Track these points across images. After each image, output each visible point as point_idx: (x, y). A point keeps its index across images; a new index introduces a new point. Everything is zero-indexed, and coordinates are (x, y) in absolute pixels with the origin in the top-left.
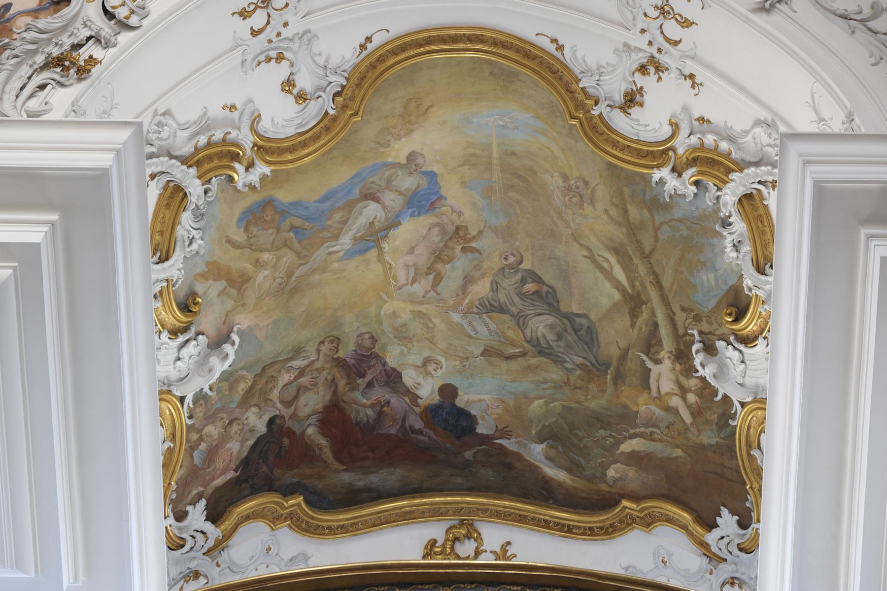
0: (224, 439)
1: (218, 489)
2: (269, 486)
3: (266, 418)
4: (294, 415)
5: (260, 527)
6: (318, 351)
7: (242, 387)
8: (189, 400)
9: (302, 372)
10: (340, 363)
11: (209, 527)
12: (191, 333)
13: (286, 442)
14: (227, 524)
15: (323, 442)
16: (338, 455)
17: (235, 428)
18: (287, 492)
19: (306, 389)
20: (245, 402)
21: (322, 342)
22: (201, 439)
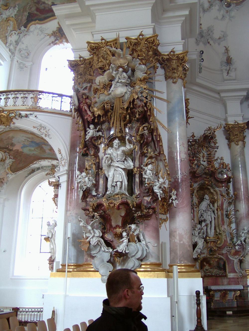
0: (22, 18)
1: (24, 24)
2: (32, 20)
3: (28, 13)
4: (31, 11)
5: (34, 26)
6: (31, 2)
7: (22, 11)
8: (14, 16)
9: (30, 6)
10: (36, 3)
11: (25, 29)
12: (10, 8)
13: (32, 15)
14: (28, 28)
15: (37, 13)
16: (40, 13)
17: (23, 16)
18: (35, 20)
19: (32, 7)
20: (23, 11)
21: (31, 1)
22: (19, 19)
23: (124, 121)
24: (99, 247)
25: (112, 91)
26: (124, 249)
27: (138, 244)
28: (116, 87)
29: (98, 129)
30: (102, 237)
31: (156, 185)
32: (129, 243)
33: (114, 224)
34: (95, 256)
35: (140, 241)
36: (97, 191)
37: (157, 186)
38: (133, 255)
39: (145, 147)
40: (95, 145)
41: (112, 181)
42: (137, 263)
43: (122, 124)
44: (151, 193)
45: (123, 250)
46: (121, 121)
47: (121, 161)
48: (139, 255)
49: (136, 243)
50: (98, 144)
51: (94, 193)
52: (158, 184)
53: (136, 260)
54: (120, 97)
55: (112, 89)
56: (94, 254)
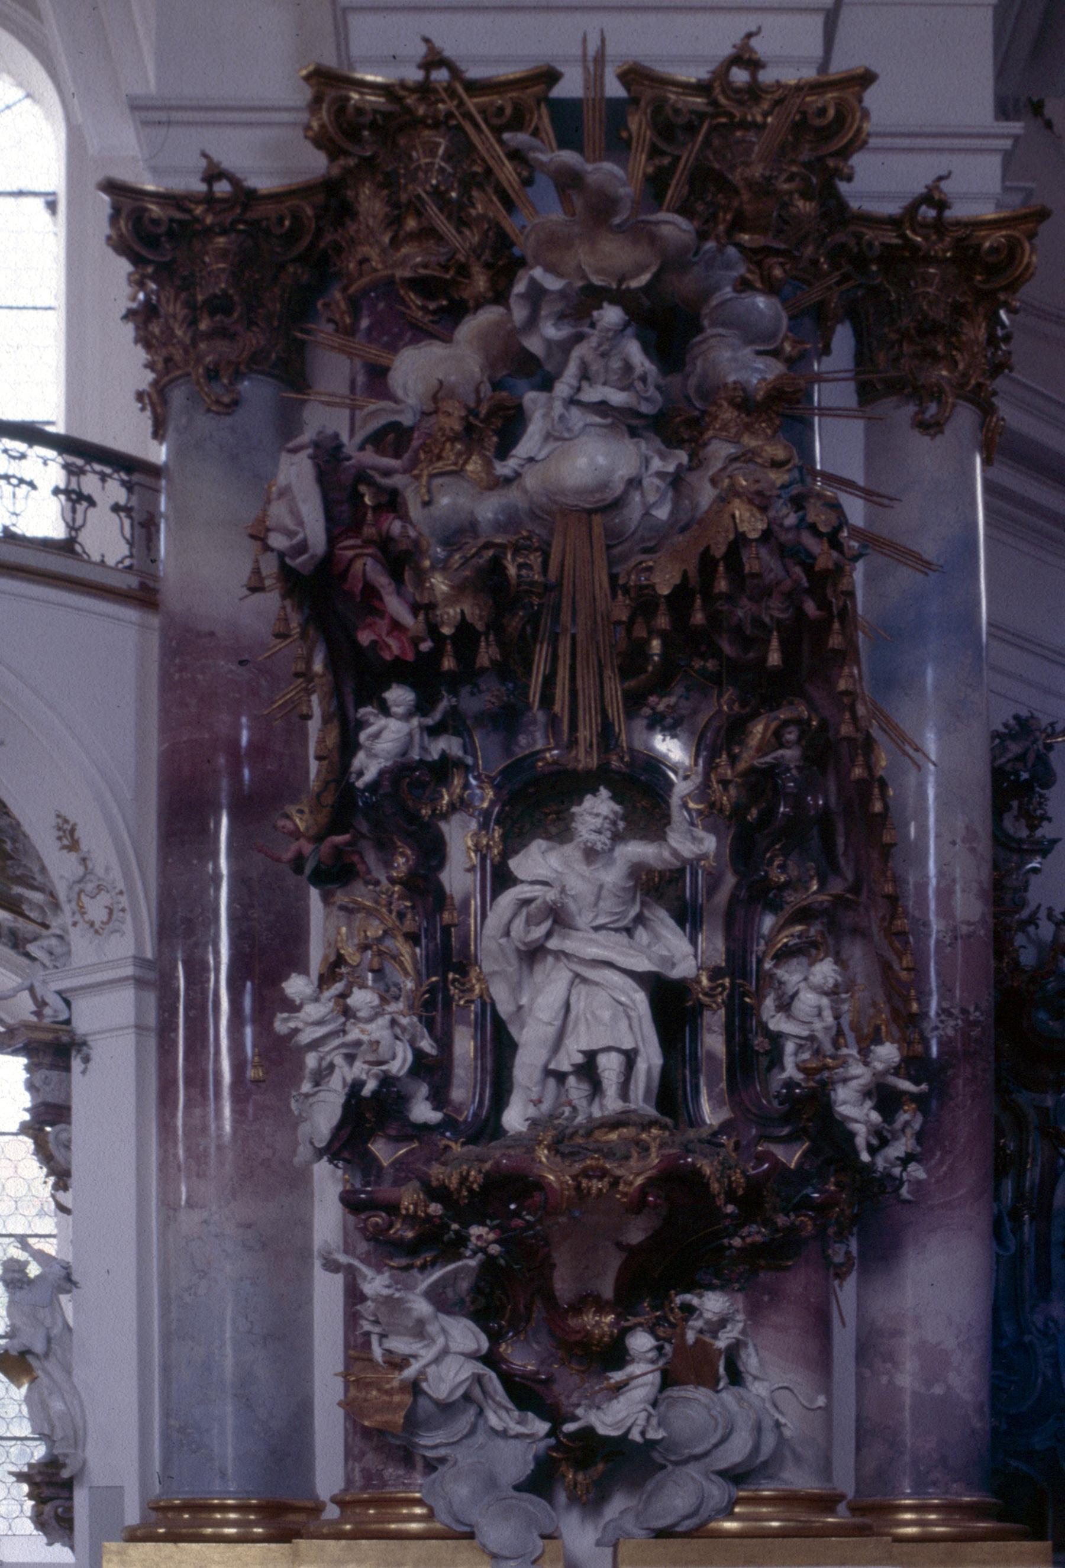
23: (625, 672)
24: (472, 1411)
25: (531, 460)
26: (641, 1422)
27: (728, 1397)
28: (557, 439)
29: (437, 715)
30: (490, 1359)
31: (845, 1081)
32: (674, 1392)
33: (563, 1286)
34: (442, 1460)
35: (736, 1377)
36: (439, 1098)
37: (854, 1084)
38: (698, 1450)
39: (777, 847)
40: (413, 817)
41: (550, 1043)
42: (717, 1492)
43: (615, 690)
44: (809, 1120)
45: (628, 1424)
46: (608, 672)
47: (616, 930)
48: (736, 1452)
49: (718, 1392)
50: (434, 810)
51: (423, 1112)
52: (860, 1074)
53: (713, 1477)
54: (590, 512)
55: (528, 445)
56: (436, 1447)
